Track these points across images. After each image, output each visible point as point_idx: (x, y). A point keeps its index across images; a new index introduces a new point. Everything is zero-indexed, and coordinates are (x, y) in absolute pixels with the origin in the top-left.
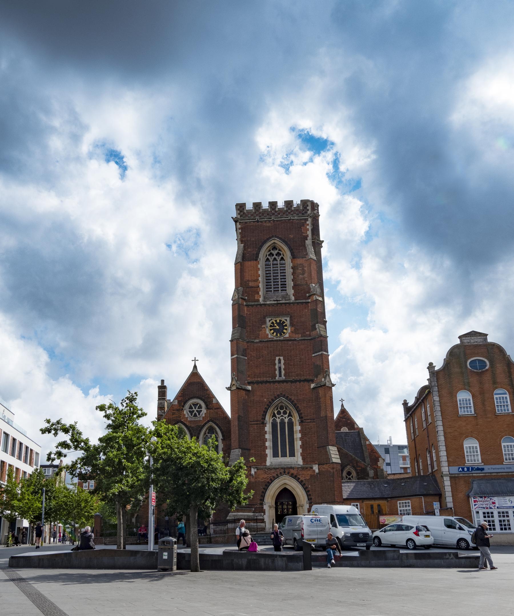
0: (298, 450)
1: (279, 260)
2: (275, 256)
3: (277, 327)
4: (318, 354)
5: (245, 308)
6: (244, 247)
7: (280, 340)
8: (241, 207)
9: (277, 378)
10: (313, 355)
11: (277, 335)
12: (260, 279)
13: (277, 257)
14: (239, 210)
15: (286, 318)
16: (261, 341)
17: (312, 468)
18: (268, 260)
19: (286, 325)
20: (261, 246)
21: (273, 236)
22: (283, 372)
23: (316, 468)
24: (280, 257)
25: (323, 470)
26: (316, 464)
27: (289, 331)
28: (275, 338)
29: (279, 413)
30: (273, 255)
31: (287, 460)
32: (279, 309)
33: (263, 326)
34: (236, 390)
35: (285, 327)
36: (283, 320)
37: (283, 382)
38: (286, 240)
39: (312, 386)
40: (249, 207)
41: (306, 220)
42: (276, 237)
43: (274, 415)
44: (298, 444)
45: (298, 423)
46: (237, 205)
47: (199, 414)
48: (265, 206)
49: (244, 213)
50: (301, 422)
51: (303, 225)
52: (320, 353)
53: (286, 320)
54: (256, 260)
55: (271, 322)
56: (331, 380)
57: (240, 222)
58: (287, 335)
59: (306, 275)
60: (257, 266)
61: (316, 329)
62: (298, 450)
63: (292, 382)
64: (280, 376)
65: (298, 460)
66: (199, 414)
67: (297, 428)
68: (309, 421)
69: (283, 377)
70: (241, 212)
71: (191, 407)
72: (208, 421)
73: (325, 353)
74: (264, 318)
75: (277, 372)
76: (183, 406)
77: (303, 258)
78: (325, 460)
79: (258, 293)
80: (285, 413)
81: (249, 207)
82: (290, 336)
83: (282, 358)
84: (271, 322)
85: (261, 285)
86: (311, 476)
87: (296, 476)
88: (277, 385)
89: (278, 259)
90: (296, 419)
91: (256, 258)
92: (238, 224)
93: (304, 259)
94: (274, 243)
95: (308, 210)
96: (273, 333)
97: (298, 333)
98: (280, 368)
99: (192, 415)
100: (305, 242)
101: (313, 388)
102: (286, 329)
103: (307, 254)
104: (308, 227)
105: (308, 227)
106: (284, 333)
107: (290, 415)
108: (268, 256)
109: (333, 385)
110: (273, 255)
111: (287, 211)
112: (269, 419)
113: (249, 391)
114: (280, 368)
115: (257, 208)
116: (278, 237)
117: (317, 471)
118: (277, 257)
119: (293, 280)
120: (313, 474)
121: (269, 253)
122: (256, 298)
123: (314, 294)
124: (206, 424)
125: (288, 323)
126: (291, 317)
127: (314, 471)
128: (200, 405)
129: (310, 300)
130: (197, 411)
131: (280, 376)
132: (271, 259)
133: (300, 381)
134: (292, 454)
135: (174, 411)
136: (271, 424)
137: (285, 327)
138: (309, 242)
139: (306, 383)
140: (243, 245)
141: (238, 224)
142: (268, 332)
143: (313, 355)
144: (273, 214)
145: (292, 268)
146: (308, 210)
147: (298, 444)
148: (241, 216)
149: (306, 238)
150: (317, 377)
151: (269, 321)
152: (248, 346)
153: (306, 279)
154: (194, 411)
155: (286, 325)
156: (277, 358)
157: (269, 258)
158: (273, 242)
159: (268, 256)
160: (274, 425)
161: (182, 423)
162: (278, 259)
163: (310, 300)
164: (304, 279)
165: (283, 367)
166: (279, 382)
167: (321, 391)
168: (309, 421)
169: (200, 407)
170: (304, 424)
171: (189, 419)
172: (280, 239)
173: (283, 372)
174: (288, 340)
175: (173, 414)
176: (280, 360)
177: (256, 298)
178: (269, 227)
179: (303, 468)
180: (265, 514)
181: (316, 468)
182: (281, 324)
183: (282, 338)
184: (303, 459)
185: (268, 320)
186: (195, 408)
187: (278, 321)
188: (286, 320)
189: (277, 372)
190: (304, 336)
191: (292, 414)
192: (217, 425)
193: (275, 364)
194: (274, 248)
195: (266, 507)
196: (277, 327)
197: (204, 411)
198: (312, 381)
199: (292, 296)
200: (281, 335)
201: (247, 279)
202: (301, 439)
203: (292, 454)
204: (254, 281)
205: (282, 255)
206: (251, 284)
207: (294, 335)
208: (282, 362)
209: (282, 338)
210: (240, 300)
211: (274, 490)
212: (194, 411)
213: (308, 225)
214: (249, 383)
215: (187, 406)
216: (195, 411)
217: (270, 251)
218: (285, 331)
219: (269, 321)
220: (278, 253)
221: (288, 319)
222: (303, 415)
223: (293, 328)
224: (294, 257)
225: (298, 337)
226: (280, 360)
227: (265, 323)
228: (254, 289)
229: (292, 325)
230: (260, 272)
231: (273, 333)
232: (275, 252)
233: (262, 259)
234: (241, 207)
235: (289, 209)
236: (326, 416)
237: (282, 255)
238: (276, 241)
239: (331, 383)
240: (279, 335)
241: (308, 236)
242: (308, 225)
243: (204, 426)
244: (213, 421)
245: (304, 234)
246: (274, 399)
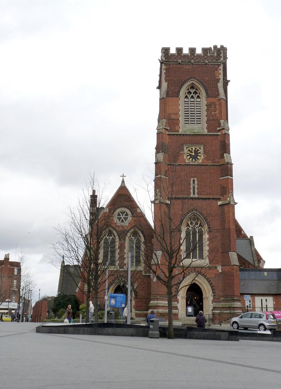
0: (206, 253)
1: (195, 98)
2: (192, 94)
3: (193, 154)
4: (225, 178)
5: (168, 137)
6: (168, 85)
7: (194, 165)
8: (166, 51)
9: (192, 196)
10: (221, 178)
11: (192, 160)
12: (180, 113)
13: (194, 95)
14: (164, 53)
15: (200, 147)
16: (179, 165)
17: (216, 268)
18: (186, 97)
19: (200, 153)
20: (182, 85)
21: (191, 78)
22: (196, 191)
23: (220, 269)
24: (197, 95)
25: (225, 270)
26: (219, 265)
27: (202, 157)
28: (191, 163)
29: (191, 223)
30: (191, 93)
31: (198, 262)
32: (194, 138)
33: (181, 152)
34: (157, 204)
35: (199, 155)
36: (198, 148)
37: (196, 198)
38: (202, 81)
39: (220, 203)
40: (173, 51)
41: (219, 65)
42: (194, 78)
43: (188, 225)
44: (206, 248)
45: (207, 233)
46: (163, 49)
48: (186, 51)
49: (168, 56)
50: (209, 232)
51: (217, 70)
52: (227, 177)
54: (178, 97)
55: (188, 149)
56: (234, 200)
57: (165, 64)
58: (200, 161)
59: (217, 112)
60: (178, 102)
61: (224, 157)
62: (206, 253)
64: (194, 194)
65: (205, 262)
67: (206, 236)
68: (215, 231)
69: (196, 196)
70: (166, 54)
73: (230, 177)
74: (182, 145)
75: (192, 191)
77: (215, 97)
78: (226, 262)
79: (178, 125)
80: (197, 224)
81: (173, 51)
82: (203, 162)
83: (195, 179)
84: (188, 149)
85: (180, 118)
86: (216, 274)
87: (203, 274)
88: (191, 202)
89: (195, 96)
90: (205, 228)
91: (177, 95)
92: (163, 65)
93: (217, 98)
94: (192, 83)
95: (221, 57)
96: (189, 159)
97: (209, 160)
98: (194, 187)
100: (217, 84)
101: (219, 205)
102: (200, 156)
103: (218, 95)
104: (220, 72)
105: (220, 72)
106: (198, 159)
107: (200, 225)
108: (186, 94)
109: (236, 204)
110: (191, 93)
111: (204, 56)
112: (184, 229)
113: (168, 204)
114: (194, 187)
115: (180, 53)
116: (196, 79)
117: (220, 271)
118: (194, 95)
119: (206, 116)
120: (217, 273)
122: (176, 129)
123: (224, 129)
125: (201, 151)
126: (204, 146)
127: (218, 271)
129: (219, 133)
131: (194, 194)
132: (189, 96)
133: (209, 199)
134: (201, 257)
136: (185, 232)
137: (199, 155)
138: (220, 85)
139: (214, 201)
140: (167, 83)
141: (163, 65)
142: (185, 158)
143: (221, 178)
144: (193, 59)
146: (221, 57)
147: (206, 248)
148: (166, 59)
149: (218, 80)
150: (223, 196)
151: (187, 148)
152: (168, 168)
153: (217, 115)
155: (200, 153)
157: (188, 95)
158: (191, 82)
159: (186, 94)
160: (188, 234)
163: (219, 133)
164: (215, 115)
165: (196, 187)
166: (192, 198)
167: (226, 208)
168: (215, 231)
170: (211, 233)
172: (198, 80)
173: (196, 191)
176: (194, 180)
177: (176, 129)
178: (188, 69)
179: (209, 268)
180: (178, 303)
181: (220, 269)
182: (196, 152)
183: (197, 163)
184: (211, 262)
185: (185, 148)
188: (200, 148)
189: (192, 191)
191: (202, 224)
193: (190, 184)
194: (192, 87)
195: (179, 297)
196: (193, 154)
198: (219, 199)
200: (195, 160)
201: (170, 112)
202: (208, 245)
203: (201, 257)
204: (175, 114)
205: (198, 94)
206: (173, 117)
208: (196, 182)
209: (196, 163)
210: (164, 130)
211: (206, 288)
213: (220, 70)
214: (169, 199)
217: (188, 89)
218: (199, 157)
219: (187, 148)
220: (195, 92)
221: (202, 148)
222: (211, 226)
223: (206, 156)
224: (208, 96)
225: (210, 163)
226: (194, 180)
227: (183, 150)
228: (175, 121)
229: (205, 152)
230: (180, 107)
231: (189, 159)
232: (192, 91)
233: (182, 96)
234: (166, 51)
235: (206, 55)
236: (229, 228)
237: (198, 94)
238: (194, 82)
239: (234, 202)
240: (194, 160)
241: (220, 79)
242: (220, 70)
245: (217, 78)
246: (188, 211)
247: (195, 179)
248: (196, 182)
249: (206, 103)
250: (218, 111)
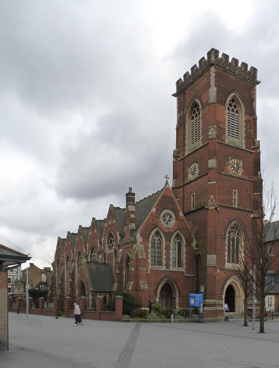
3: (235, 166)
28: (234, 175)
63: (241, 210)
69: (236, 206)
76: (160, 215)
83: (237, 191)
98: (235, 198)
106: (239, 172)
124: (175, 231)
131: (235, 205)
135: (153, 217)
145: (245, 122)
154: (168, 220)
156: (234, 190)
161: (159, 227)
165: (237, 198)
175: (153, 219)
176: (235, 192)
208: (237, 194)
209: (237, 176)
212: (168, 220)
215: (162, 215)
226: (235, 192)
243: (174, 232)
247: (237, 191)
248: (237, 194)
249: (244, 119)
250: (253, 130)
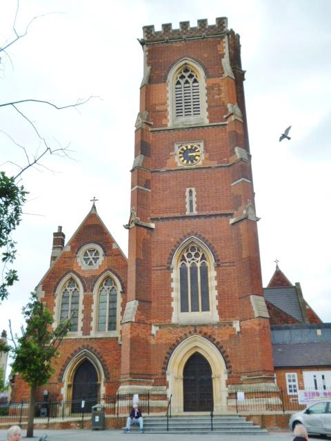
18: (178, 83)
27: (203, 158)
47: (95, 262)
51: (219, 43)
53: (199, 146)
66: (95, 262)
71: (86, 254)
72: (106, 270)
76: (77, 253)
89: (191, 81)
97: (214, 160)
99: (86, 263)
105: (224, 45)
121: (180, 75)
124: (102, 273)
128: (97, 252)
129: (227, 123)
130: (93, 258)
154: (89, 258)
158: (184, 62)
162: (191, 81)
163: (227, 123)
169: (97, 253)
171: (83, 268)
174: (201, 168)
186: (91, 255)
187: (189, 147)
188: (199, 146)
190: (221, 163)
192: (116, 275)
194: (186, 71)
197: (101, 258)
199: (206, 118)
207: (209, 161)
212: (89, 258)
213: (225, 42)
216: (91, 259)
221: (202, 144)
237: (195, 77)
238: (187, 62)
241: (224, 54)
242: (225, 42)
243: (100, 276)
244: (111, 270)
